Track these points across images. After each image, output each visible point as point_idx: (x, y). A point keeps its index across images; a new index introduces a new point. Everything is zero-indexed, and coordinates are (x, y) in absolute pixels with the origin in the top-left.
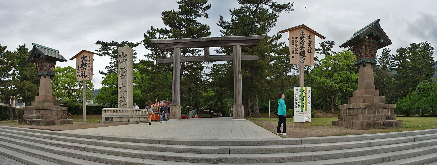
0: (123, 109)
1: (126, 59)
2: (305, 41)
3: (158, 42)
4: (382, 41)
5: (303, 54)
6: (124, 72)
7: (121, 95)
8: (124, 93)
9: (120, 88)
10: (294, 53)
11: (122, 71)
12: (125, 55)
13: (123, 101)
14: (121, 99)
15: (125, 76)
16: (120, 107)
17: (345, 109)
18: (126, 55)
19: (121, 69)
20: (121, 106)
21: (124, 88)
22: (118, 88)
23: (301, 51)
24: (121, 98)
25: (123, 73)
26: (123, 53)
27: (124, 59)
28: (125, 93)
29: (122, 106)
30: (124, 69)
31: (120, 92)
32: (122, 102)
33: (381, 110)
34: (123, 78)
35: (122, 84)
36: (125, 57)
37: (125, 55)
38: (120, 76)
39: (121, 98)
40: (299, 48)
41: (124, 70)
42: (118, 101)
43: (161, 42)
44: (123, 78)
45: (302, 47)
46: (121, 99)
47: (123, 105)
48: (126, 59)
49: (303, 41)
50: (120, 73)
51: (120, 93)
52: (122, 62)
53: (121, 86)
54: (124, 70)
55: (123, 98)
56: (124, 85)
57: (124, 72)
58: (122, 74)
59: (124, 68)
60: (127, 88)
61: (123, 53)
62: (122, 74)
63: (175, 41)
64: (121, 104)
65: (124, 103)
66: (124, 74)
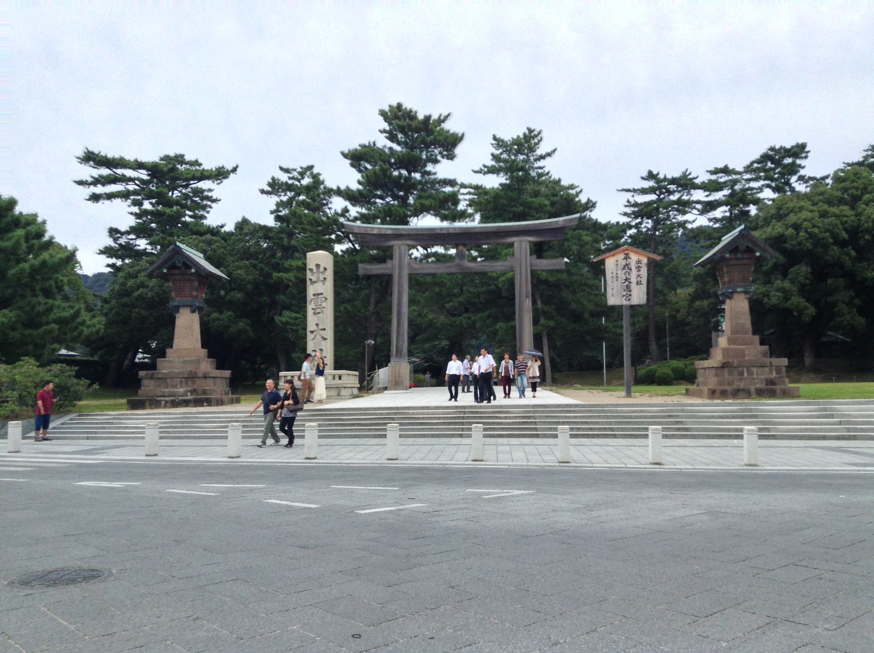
2: (631, 269)
7: (315, 346)
9: (312, 332)
12: (322, 269)
15: (323, 309)
18: (325, 269)
19: (314, 295)
22: (308, 333)
23: (625, 284)
24: (314, 351)
25: (318, 303)
26: (318, 266)
27: (321, 277)
28: (323, 342)
31: (314, 339)
34: (319, 313)
35: (317, 325)
36: (322, 272)
37: (322, 269)
38: (313, 309)
39: (314, 351)
43: (367, 230)
44: (319, 313)
48: (324, 276)
49: (629, 271)
50: (313, 302)
51: (312, 342)
52: (315, 282)
54: (321, 298)
56: (321, 327)
58: (316, 306)
59: (322, 294)
61: (318, 266)
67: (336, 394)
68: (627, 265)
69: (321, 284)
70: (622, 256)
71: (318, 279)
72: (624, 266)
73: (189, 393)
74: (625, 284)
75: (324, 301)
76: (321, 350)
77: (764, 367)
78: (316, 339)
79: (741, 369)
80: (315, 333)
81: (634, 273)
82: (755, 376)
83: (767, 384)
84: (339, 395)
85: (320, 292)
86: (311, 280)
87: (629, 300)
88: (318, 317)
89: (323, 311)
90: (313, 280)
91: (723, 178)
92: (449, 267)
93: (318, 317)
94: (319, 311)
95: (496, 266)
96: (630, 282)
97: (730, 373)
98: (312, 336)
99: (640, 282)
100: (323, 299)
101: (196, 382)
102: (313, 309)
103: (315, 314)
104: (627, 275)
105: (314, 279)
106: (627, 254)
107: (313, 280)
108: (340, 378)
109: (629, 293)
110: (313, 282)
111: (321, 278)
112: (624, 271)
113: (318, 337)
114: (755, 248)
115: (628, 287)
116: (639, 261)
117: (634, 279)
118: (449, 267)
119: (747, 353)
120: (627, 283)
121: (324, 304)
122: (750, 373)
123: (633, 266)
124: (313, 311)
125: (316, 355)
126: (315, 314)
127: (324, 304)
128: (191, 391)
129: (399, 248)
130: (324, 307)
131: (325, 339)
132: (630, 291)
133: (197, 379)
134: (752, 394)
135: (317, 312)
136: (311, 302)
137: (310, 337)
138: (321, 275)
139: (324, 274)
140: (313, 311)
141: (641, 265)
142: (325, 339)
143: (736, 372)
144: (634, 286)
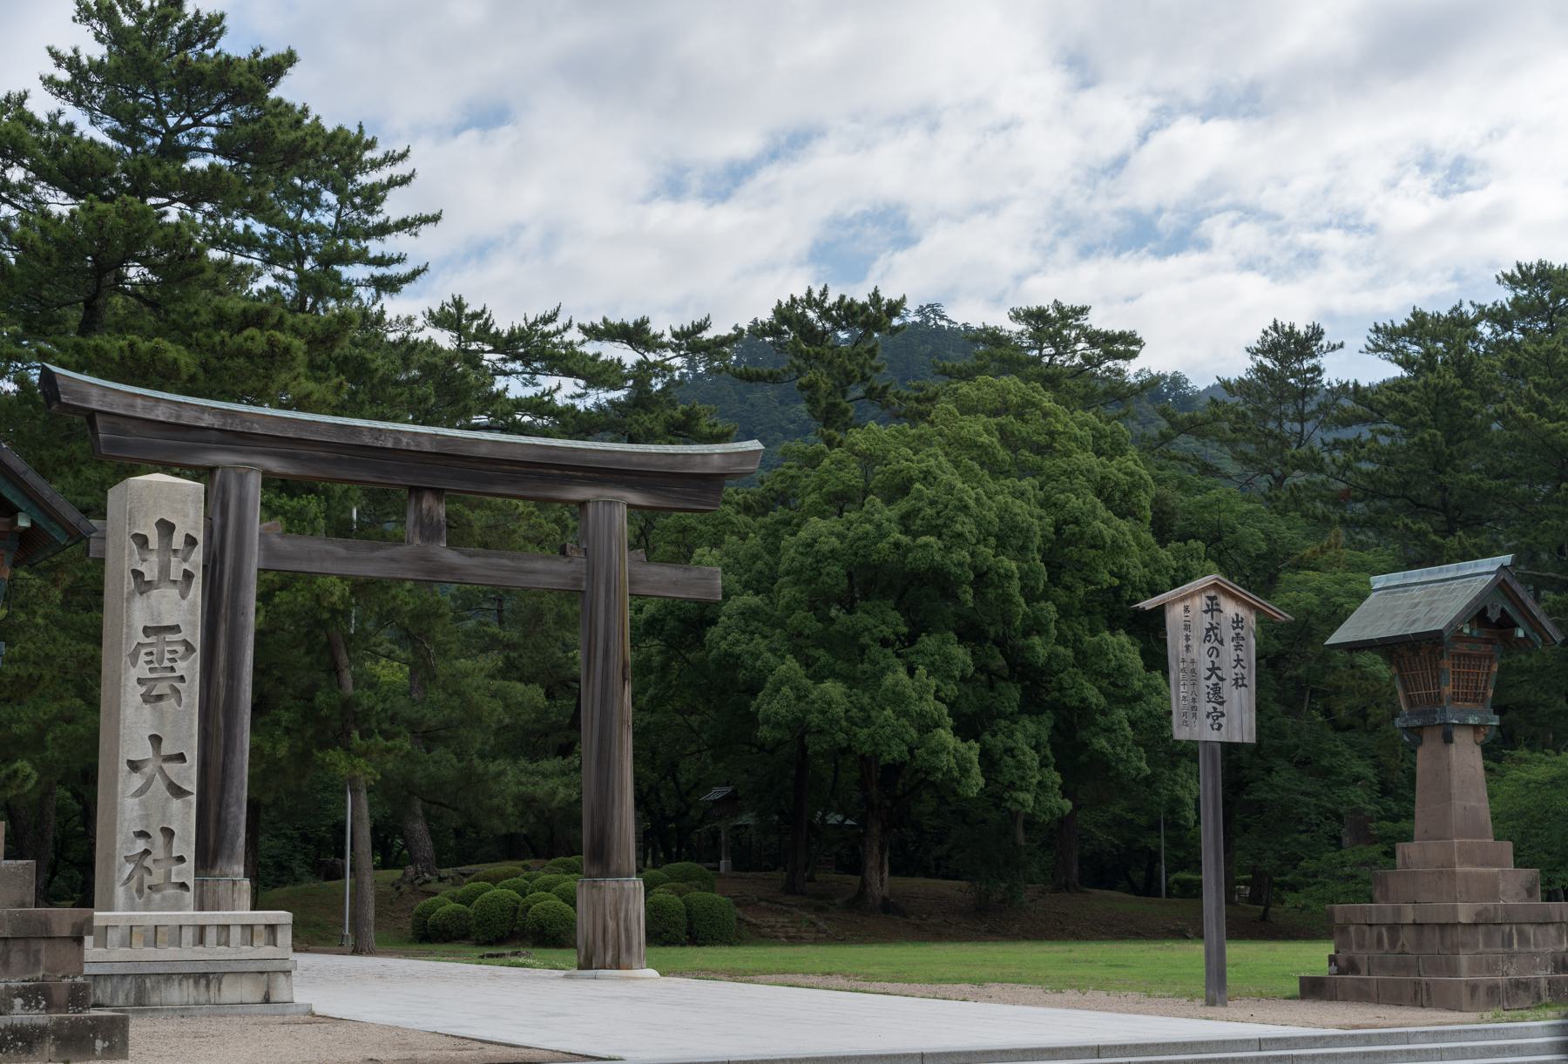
1: (185, 571)
2: (1221, 642)
3: (111, 405)
4: (1521, 633)
6: (173, 660)
8: (167, 800)
9: (134, 766)
13: (155, 861)
14: (141, 845)
15: (178, 685)
16: (133, 899)
18: (191, 541)
19: (147, 631)
20: (140, 891)
21: (172, 769)
23: (1210, 683)
24: (142, 834)
25: (161, 661)
26: (166, 528)
28: (176, 804)
29: (146, 891)
30: (170, 637)
31: (141, 792)
32: (148, 862)
33: (1530, 930)
34: (160, 698)
35: (156, 740)
37: (178, 541)
38: (140, 681)
39: (142, 834)
42: (120, 859)
44: (160, 698)
46: (141, 845)
48: (186, 566)
49: (1216, 644)
50: (143, 658)
51: (136, 800)
55: (159, 839)
56: (167, 748)
57: (173, 660)
58: (151, 670)
59: (175, 629)
60: (191, 767)
61: (166, 528)
64: (141, 883)
65: (168, 874)
66: (172, 669)
67: (259, 997)
68: (1212, 628)
69: (174, 593)
70: (1199, 603)
71: (164, 570)
72: (1208, 630)
73: (18, 1002)
74: (1210, 683)
75: (183, 658)
76: (168, 833)
77: (1546, 924)
78: (148, 793)
79: (1507, 928)
81: (1229, 651)
82: (1533, 949)
83: (1556, 970)
84: (267, 1000)
85: (165, 624)
86: (137, 574)
87: (1220, 726)
88: (162, 714)
89: (176, 691)
90: (147, 578)
91: (628, 356)
92: (392, 560)
93: (162, 714)
96: (1222, 679)
97: (1489, 942)
98: (137, 781)
99: (1243, 678)
100: (181, 649)
101: (43, 957)
102: (140, 681)
103: (147, 699)
104: (1213, 658)
105: (150, 571)
106: (1209, 598)
107: (147, 578)
109: (1219, 708)
110: (143, 584)
111: (176, 573)
112: (1208, 645)
113: (159, 785)
114: (1518, 619)
115: (1216, 689)
116: (1238, 622)
117: (1229, 673)
118: (392, 560)
119: (1501, 887)
120: (1214, 679)
122: (1524, 939)
123: (1228, 633)
125: (147, 852)
126: (147, 699)
127: (181, 667)
128: (25, 993)
129: (241, 480)
130: (182, 678)
131: (177, 791)
132: (1221, 703)
133: (43, 945)
134: (1543, 994)
136: (134, 656)
139: (185, 560)
140: (143, 689)
141: (1242, 633)
142: (177, 791)
143: (1498, 939)
144: (1227, 689)
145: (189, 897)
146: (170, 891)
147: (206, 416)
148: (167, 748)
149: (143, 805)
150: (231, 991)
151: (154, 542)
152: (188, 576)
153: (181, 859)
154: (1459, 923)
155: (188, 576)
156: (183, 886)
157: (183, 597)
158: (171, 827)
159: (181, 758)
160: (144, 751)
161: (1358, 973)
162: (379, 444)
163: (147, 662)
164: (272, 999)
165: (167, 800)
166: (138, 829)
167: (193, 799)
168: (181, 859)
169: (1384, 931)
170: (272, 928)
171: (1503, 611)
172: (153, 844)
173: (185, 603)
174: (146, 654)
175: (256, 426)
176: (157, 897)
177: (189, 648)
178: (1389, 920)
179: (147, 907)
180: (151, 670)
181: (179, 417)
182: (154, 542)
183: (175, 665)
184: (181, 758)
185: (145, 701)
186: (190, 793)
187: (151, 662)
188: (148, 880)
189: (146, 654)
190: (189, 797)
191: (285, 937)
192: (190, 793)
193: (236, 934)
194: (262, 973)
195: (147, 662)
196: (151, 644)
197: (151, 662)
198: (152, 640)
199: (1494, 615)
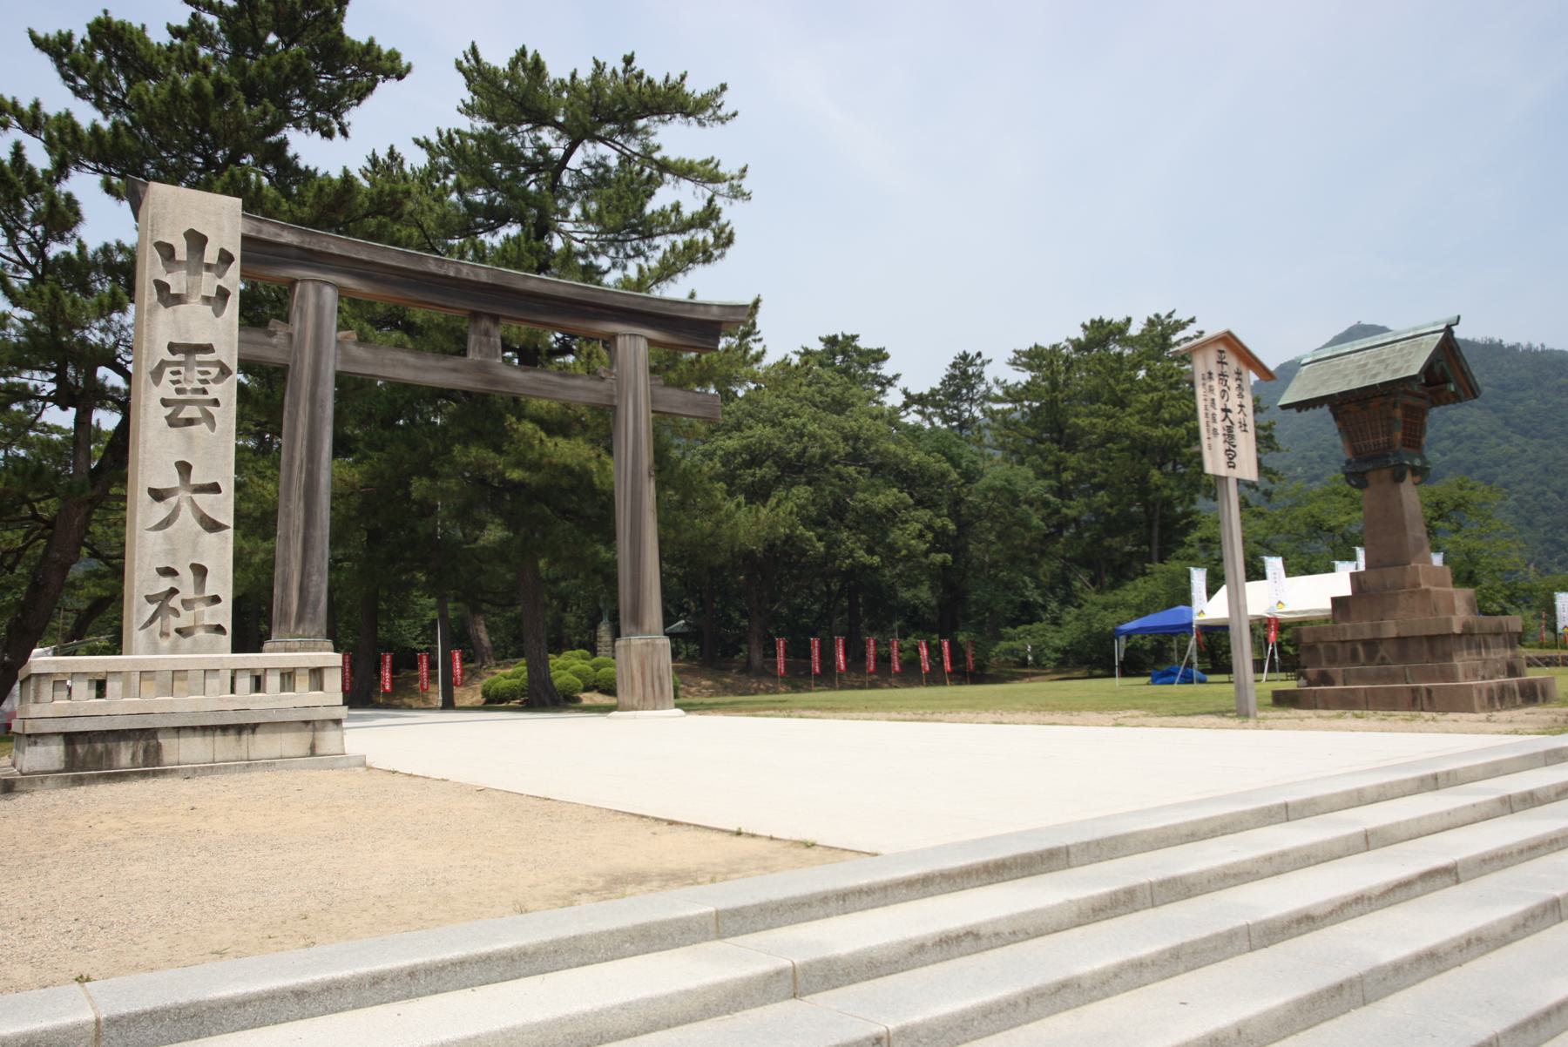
0: (165, 660)
1: (219, 287)
5: (1230, 429)
6: (205, 382)
7: (172, 552)
8: (198, 534)
9: (158, 495)
10: (1211, 429)
11: (182, 369)
13: (184, 602)
14: (166, 584)
15: (211, 409)
16: (155, 643)
17: (1343, 642)
19: (173, 348)
21: (205, 501)
24: (169, 572)
29: (174, 634)
30: (200, 357)
31: (166, 523)
32: (175, 602)
34: (190, 422)
35: (184, 468)
36: (209, 267)
37: (211, 255)
38: (165, 403)
39: (169, 572)
40: (1220, 415)
41: (201, 364)
44: (190, 422)
45: (1226, 410)
46: (166, 584)
47: (179, 631)
48: (220, 282)
50: (167, 375)
51: (160, 533)
53: (168, 478)
54: (201, 364)
55: (187, 576)
56: (197, 478)
57: (205, 382)
59: (208, 349)
60: (228, 497)
61: (197, 241)
62: (179, 391)
63: (314, 241)
66: (205, 392)
67: (305, 749)
75: (216, 381)
76: (200, 571)
78: (175, 525)
80: (173, 500)
86: (162, 287)
88: (190, 438)
94: (189, 412)
95: (574, 388)
98: (161, 511)
100: (215, 371)
102: (165, 403)
103: (173, 422)
108: (100, 688)
113: (187, 518)
118: (455, 370)
121: (215, 391)
124: (169, 411)
125: (173, 591)
126: (173, 422)
127: (215, 391)
129: (319, 293)
130: (216, 402)
131: (213, 526)
135: (183, 415)
136: (157, 374)
137: (143, 513)
138: (207, 276)
139: (220, 277)
140: (169, 411)
142: (213, 526)
144: (1237, 431)
145: (226, 640)
146: (200, 634)
147: (285, 234)
148: (197, 478)
149: (168, 538)
150: (263, 745)
151: (182, 253)
152: (223, 294)
153: (216, 599)
154: (1454, 634)
155: (223, 294)
156: (219, 629)
157: (217, 314)
158: (203, 563)
159: (215, 488)
160: (168, 478)
161: (1333, 684)
162: (442, 272)
163: (174, 382)
164: (318, 751)
165: (198, 534)
166: (163, 565)
167: (230, 533)
168: (216, 599)
169: (1360, 649)
170: (317, 673)
171: (1442, 368)
172: (181, 582)
173: (219, 320)
174: (173, 373)
175: (332, 246)
176: (187, 642)
177: (225, 371)
178: (1368, 635)
179: (174, 649)
180: (179, 391)
181: (260, 231)
182: (182, 253)
183: (206, 386)
184: (215, 488)
185: (171, 425)
186: (226, 527)
187: (178, 382)
188: (175, 622)
189: (173, 373)
190: (226, 531)
191: (334, 683)
192: (226, 527)
193: (273, 682)
194: (307, 722)
195: (174, 382)
196: (179, 363)
197: (178, 382)
198: (180, 357)
199: (1437, 369)
